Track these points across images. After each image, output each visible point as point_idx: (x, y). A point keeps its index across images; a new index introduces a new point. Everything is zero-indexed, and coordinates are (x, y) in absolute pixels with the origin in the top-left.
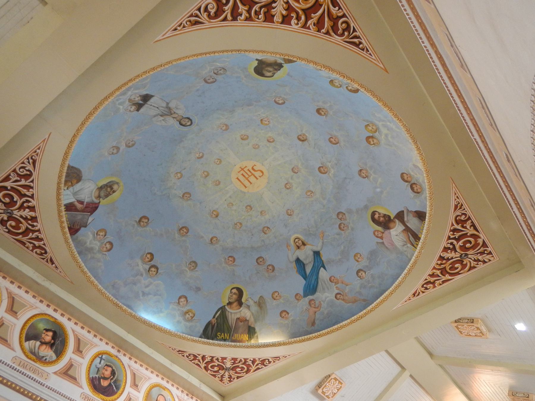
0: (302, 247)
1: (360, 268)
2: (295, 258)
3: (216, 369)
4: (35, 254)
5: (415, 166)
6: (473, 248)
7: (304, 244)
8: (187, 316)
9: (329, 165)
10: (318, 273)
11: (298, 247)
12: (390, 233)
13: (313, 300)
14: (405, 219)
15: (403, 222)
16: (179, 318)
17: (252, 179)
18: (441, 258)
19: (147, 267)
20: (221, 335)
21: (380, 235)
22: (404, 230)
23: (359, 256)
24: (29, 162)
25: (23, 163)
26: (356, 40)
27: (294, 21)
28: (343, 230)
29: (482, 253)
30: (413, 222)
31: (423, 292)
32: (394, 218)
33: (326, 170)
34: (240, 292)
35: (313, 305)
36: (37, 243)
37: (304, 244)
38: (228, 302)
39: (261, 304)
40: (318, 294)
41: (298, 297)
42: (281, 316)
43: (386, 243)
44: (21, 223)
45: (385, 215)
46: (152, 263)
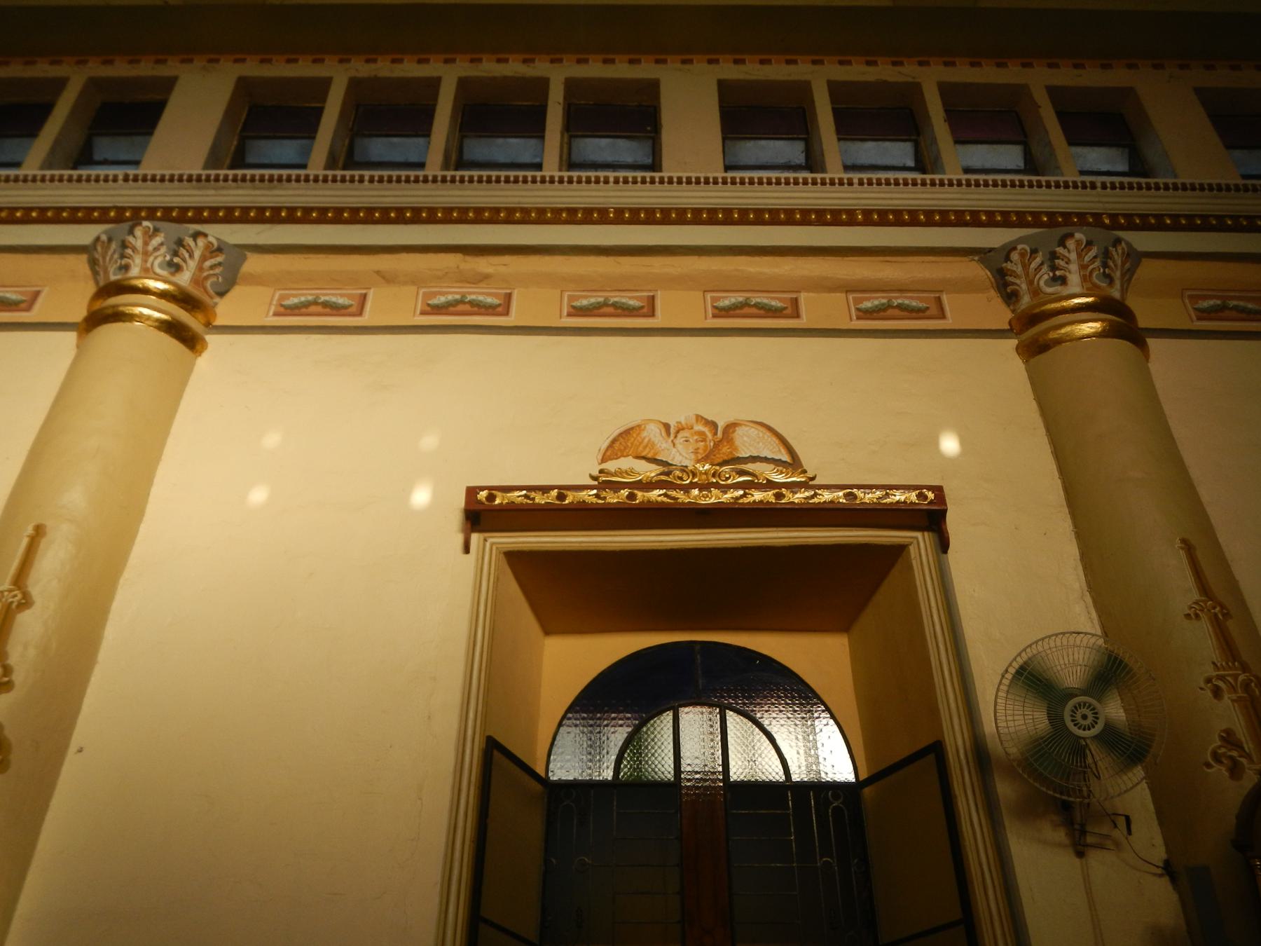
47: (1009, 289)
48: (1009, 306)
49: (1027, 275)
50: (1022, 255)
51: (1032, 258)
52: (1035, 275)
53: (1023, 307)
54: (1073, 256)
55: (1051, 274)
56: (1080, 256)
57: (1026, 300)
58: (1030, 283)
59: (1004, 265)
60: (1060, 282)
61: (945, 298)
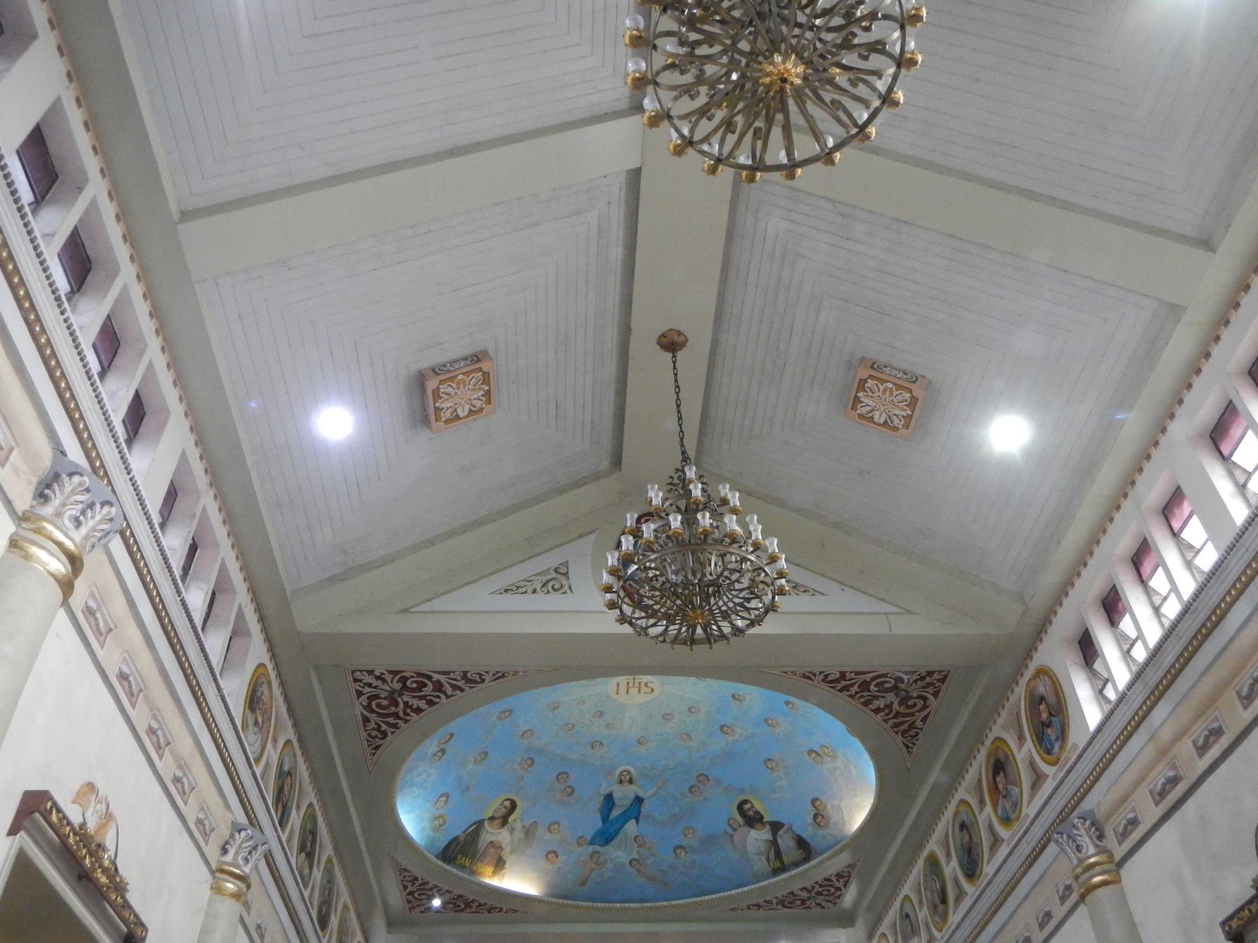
0: (627, 784)
1: (684, 844)
2: (607, 791)
3: (422, 897)
4: (365, 734)
5: (839, 807)
6: (826, 895)
7: (631, 781)
8: (436, 822)
9: (739, 731)
10: (626, 823)
11: (621, 782)
12: (749, 832)
13: (598, 853)
14: (781, 832)
15: (775, 833)
16: (426, 824)
17: (633, 691)
18: (792, 893)
19: (438, 749)
20: (461, 859)
21: (734, 826)
22: (766, 841)
23: (691, 831)
24: (494, 675)
25: (488, 672)
26: (911, 745)
27: (883, 714)
28: (692, 793)
29: (829, 901)
30: (785, 842)
31: (742, 910)
32: (767, 822)
33: (729, 732)
34: (513, 806)
35: (595, 860)
36: (384, 727)
37: (631, 781)
38: (491, 815)
39: (529, 832)
40: (609, 849)
41: (581, 841)
42: (546, 856)
43: (736, 839)
44: (397, 705)
45: (759, 812)
46: (444, 746)
47: (47, 491)
48: (34, 499)
49: (68, 498)
50: (80, 484)
51: (81, 493)
52: (71, 504)
53: (41, 513)
54: (98, 517)
55: (78, 514)
56: (100, 522)
57: (48, 510)
58: (64, 505)
59: (64, 476)
60: (76, 524)
61: (15, 453)
